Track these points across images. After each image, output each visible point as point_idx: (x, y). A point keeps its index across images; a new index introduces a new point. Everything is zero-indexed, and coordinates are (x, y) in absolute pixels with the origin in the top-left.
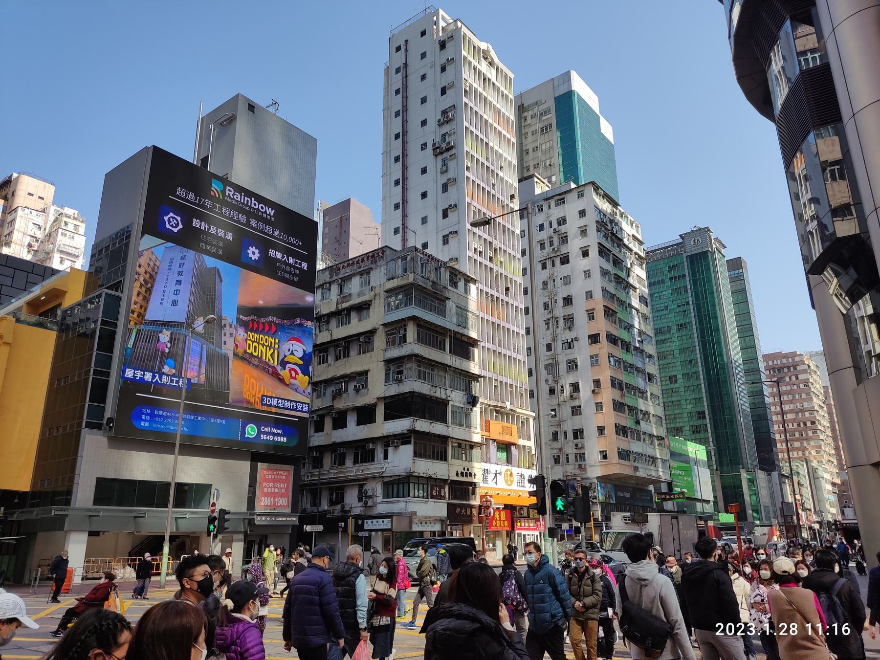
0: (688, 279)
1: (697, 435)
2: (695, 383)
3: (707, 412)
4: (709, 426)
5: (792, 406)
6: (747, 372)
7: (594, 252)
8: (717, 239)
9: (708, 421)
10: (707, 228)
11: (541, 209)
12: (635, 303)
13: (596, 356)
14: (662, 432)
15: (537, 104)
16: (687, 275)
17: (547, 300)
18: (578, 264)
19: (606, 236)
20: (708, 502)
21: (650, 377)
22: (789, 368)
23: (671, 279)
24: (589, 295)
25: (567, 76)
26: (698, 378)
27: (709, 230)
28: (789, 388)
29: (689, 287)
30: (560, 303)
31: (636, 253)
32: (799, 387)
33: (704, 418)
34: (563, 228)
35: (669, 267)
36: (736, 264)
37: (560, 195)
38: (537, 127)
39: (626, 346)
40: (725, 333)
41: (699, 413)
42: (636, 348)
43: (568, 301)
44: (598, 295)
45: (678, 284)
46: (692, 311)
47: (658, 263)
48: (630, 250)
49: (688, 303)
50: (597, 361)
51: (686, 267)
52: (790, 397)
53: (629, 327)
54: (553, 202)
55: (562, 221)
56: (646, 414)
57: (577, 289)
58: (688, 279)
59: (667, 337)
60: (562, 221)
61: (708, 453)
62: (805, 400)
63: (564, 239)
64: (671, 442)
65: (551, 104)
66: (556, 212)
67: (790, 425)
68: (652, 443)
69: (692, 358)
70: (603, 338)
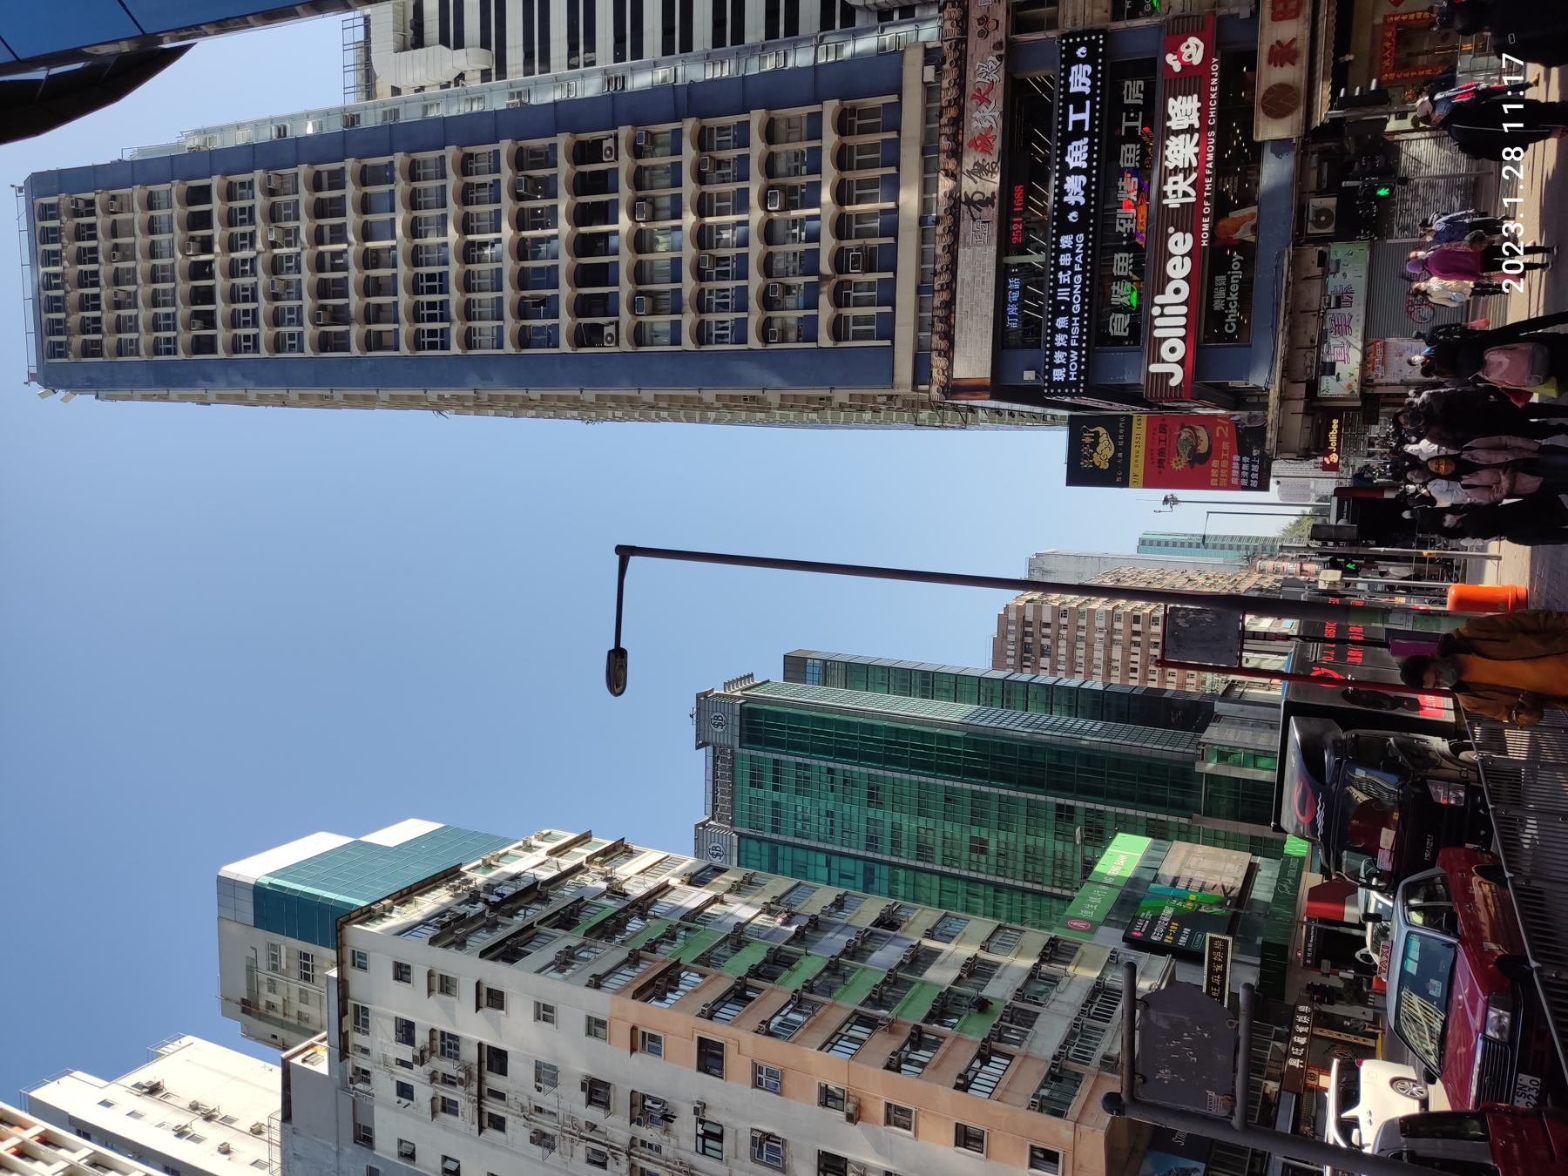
0: (783, 757)
1: (1099, 837)
2: (995, 805)
3: (1061, 801)
4: (1090, 806)
5: (1099, 646)
6: (1006, 703)
7: (498, 974)
8: (727, 685)
9: (1080, 804)
10: (698, 696)
11: (364, 1075)
12: (694, 898)
13: (757, 1069)
14: (1036, 939)
15: (251, 969)
16: (776, 756)
17: (581, 1150)
18: (516, 1031)
19: (492, 926)
20: (1252, 870)
21: (889, 922)
22: (1026, 634)
23: (775, 788)
24: (595, 1027)
25: (228, 887)
26: (986, 796)
27: (705, 695)
28: (1062, 643)
29: (800, 760)
30: (595, 1114)
31: (590, 860)
32: (1065, 627)
33: (1071, 809)
34: (421, 1037)
35: (752, 784)
36: (796, 667)
37: (343, 1012)
38: (296, 985)
39: (776, 964)
40: (906, 719)
41: (1059, 817)
42: (799, 937)
43: (596, 1091)
44: (601, 1003)
45: (789, 777)
46: (848, 767)
47: (738, 803)
48: (578, 868)
49: (830, 771)
50: (771, 1073)
51: (761, 754)
52: (1081, 645)
53: (739, 937)
54: (356, 1039)
55: (406, 1031)
56: (976, 970)
57: (579, 1058)
58: (783, 757)
59: (888, 830)
60: (406, 1031)
61: (1130, 827)
62: (1091, 623)
63: (448, 1044)
64: (1084, 913)
65: (263, 937)
66: (381, 1042)
67: (1133, 658)
68: (1053, 981)
69: (941, 796)
70: (715, 1031)
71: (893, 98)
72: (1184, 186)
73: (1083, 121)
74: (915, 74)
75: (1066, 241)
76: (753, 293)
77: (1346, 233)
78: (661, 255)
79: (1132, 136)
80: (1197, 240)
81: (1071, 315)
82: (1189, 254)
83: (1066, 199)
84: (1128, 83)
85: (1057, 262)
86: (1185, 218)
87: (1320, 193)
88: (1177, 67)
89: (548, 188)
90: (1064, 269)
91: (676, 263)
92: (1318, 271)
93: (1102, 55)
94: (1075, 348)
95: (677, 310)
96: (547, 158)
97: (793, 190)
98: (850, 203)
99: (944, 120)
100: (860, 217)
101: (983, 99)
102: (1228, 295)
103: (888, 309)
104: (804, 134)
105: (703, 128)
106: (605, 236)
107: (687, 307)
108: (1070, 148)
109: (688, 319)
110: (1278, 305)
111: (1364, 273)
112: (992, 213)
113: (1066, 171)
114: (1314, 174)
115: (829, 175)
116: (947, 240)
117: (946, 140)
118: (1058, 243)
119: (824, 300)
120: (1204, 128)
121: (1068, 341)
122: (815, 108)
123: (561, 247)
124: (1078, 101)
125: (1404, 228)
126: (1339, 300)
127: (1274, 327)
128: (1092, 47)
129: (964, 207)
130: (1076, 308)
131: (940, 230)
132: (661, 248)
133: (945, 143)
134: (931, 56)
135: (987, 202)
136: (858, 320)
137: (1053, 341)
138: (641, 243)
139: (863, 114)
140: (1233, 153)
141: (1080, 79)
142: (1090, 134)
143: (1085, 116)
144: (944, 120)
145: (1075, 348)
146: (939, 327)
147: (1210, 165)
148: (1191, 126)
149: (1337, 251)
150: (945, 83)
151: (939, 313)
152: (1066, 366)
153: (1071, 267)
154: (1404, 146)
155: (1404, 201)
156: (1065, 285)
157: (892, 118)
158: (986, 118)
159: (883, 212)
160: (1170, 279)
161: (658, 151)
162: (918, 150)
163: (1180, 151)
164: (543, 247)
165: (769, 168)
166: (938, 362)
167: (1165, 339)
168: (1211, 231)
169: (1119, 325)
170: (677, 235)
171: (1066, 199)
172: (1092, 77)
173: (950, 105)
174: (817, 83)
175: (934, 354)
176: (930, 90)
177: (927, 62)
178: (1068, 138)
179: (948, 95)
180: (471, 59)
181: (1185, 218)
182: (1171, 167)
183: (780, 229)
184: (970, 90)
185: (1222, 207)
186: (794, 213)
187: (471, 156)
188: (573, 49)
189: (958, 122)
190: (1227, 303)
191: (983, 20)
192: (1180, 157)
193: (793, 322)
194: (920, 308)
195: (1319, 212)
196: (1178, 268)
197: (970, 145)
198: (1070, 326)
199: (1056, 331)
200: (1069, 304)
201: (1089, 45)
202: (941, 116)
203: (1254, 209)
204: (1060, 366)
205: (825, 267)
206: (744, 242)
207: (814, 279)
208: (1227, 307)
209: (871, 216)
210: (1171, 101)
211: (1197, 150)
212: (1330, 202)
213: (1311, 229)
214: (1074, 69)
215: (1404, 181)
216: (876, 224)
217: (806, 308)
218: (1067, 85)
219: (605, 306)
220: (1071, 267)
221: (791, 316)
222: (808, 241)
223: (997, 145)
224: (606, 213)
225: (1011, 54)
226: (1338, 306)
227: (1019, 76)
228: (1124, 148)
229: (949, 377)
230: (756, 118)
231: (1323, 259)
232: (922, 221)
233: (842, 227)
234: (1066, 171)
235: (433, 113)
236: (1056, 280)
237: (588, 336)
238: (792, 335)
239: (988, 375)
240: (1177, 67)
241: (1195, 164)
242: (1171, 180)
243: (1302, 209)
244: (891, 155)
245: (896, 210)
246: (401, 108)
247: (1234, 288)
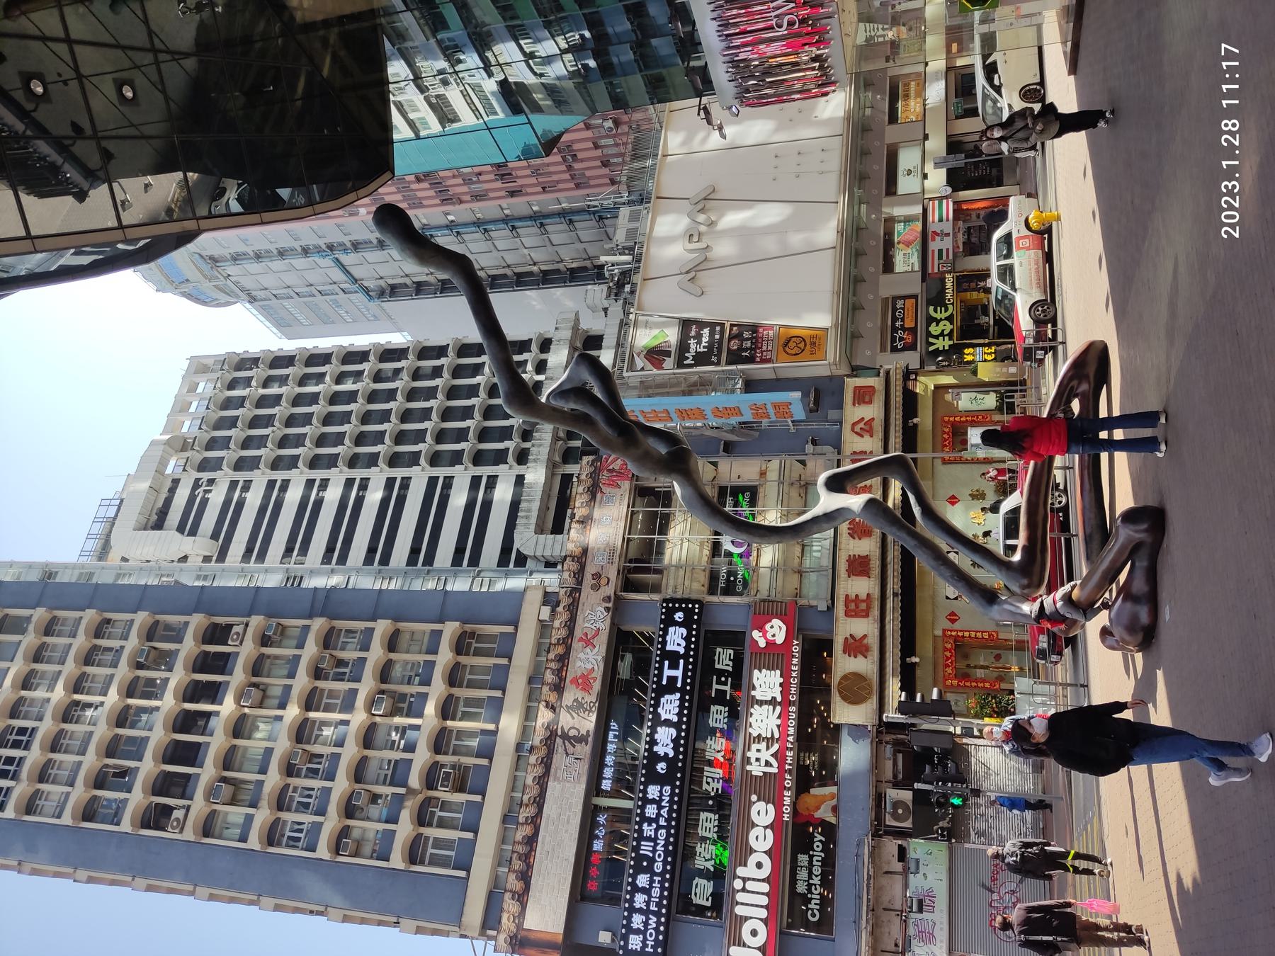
71: (510, 629)
72: (766, 755)
73: (676, 678)
74: (533, 612)
75: (653, 791)
76: (335, 798)
77: (922, 830)
78: (254, 745)
79: (720, 699)
80: (779, 813)
81: (653, 874)
82: (771, 826)
83: (655, 749)
84: (719, 650)
85: (643, 812)
86: (768, 788)
87: (896, 785)
88: (762, 643)
89: (165, 660)
90: (650, 821)
91: (269, 752)
92: (898, 866)
93: (697, 622)
94: (654, 913)
95: (254, 805)
96: (176, 635)
97: (403, 697)
98: (453, 719)
99: (551, 656)
100: (461, 734)
101: (588, 642)
102: (810, 878)
103: (470, 835)
104: (424, 648)
105: (332, 628)
106: (207, 715)
107: (264, 803)
108: (663, 700)
109: (263, 816)
110: (860, 898)
111: (944, 876)
112: (585, 750)
113: (658, 722)
114: (889, 764)
115: (438, 689)
116: (539, 771)
117: (552, 676)
118: (645, 792)
119: (406, 816)
120: (786, 703)
121: (648, 903)
122: (370, 624)
123: (159, 720)
124: (673, 658)
125: (981, 834)
126: (920, 902)
127: (857, 922)
128: (688, 613)
129: (559, 741)
130: (658, 867)
131: (533, 759)
132: (258, 735)
133: (549, 677)
134: (549, 599)
135: (581, 739)
136: (438, 843)
137: (631, 901)
138: (240, 728)
139: (480, 638)
140: (813, 733)
141: (676, 639)
142: (682, 691)
143: (678, 673)
144: (551, 656)
145: (654, 913)
146: (517, 864)
147: (791, 739)
148: (774, 698)
149: (918, 847)
150: (557, 624)
151: (520, 848)
152: (644, 933)
153: (656, 820)
154: (972, 750)
155: (978, 806)
156: (649, 839)
157: (506, 648)
158: (589, 660)
159: (484, 732)
160: (752, 851)
161: (285, 642)
162: (524, 679)
163: (763, 721)
164: (144, 717)
165: (385, 674)
166: (510, 905)
167: (747, 918)
168: (794, 805)
169: (702, 891)
170: (278, 725)
171: (655, 749)
172: (687, 639)
173: (558, 643)
174: (444, 607)
175: (508, 896)
176: (544, 627)
177: (545, 603)
178: (662, 691)
179: (558, 633)
180: (199, 546)
181: (768, 788)
182: (755, 735)
183: (380, 736)
184: (578, 633)
185: (804, 782)
186: (398, 720)
187: (108, 621)
188: (289, 551)
189: (563, 659)
190: (810, 886)
191: (597, 576)
192: (763, 726)
193: (371, 835)
194: (503, 840)
195: (896, 804)
196: (761, 840)
197: (571, 682)
198: (651, 887)
199: (636, 889)
200: (652, 861)
201: (685, 610)
202: (548, 652)
203: (834, 789)
204: (637, 932)
205: (414, 781)
206: (340, 743)
207: (402, 791)
208: (809, 891)
209: (472, 734)
210: (756, 672)
211: (779, 722)
212: (907, 796)
213: (890, 821)
214: (671, 629)
215: (977, 793)
216: (474, 743)
217: (387, 822)
218: (664, 643)
219: (185, 787)
220: (656, 820)
221: (367, 828)
222: (404, 750)
223: (597, 686)
224: (212, 692)
225: (617, 608)
226: (920, 910)
227: (625, 628)
228: (714, 708)
229: (519, 926)
230: (382, 627)
231: (902, 854)
232: (519, 747)
233: (440, 742)
234: (658, 722)
235: (125, 581)
236: (640, 831)
237: (156, 817)
238: (367, 849)
239: (560, 929)
240: (762, 643)
241: (777, 735)
242: (754, 747)
243: (879, 798)
244: (499, 681)
245: (495, 733)
246: (97, 572)
247: (817, 870)
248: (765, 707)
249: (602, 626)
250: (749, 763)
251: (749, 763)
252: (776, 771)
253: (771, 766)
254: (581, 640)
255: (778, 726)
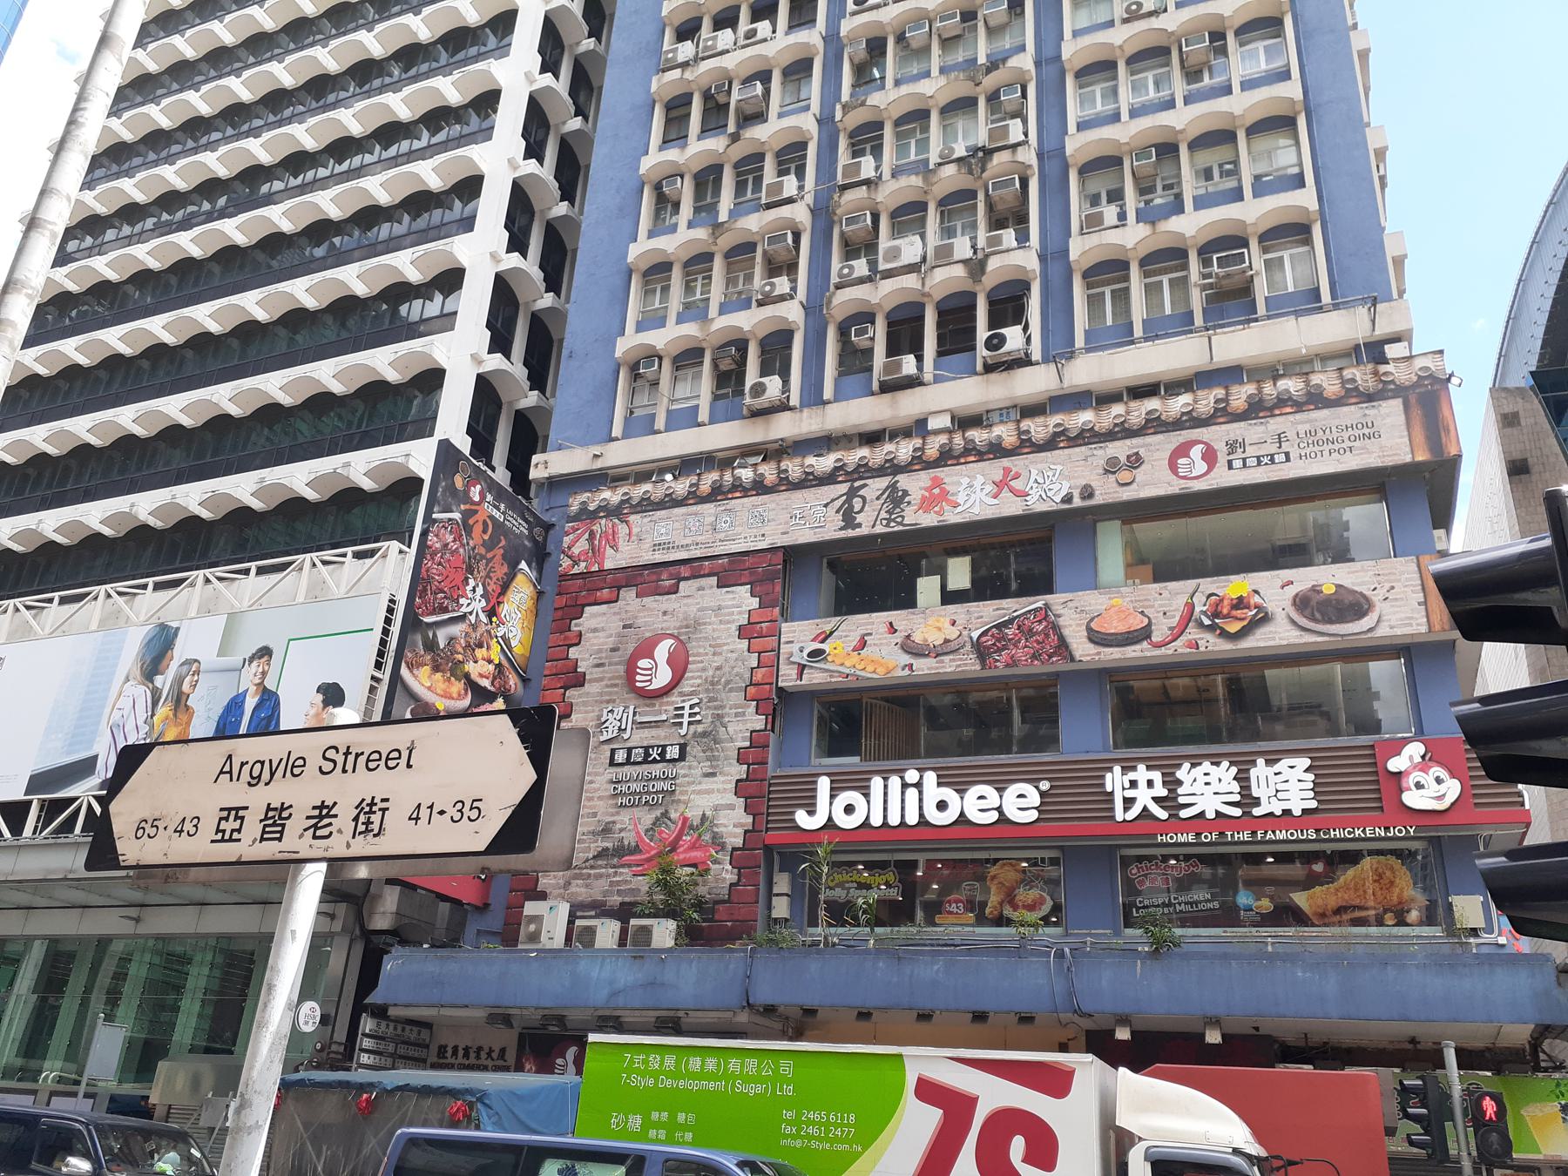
148: (1257, 802)
192: (1199, 787)
211: (1210, 815)
242: (1157, 776)
248: (1235, 787)
249: (1031, 500)
250: (1125, 770)
251: (1125, 770)
252: (1119, 818)
253: (1126, 809)
254: (1007, 471)
255: (1202, 814)
